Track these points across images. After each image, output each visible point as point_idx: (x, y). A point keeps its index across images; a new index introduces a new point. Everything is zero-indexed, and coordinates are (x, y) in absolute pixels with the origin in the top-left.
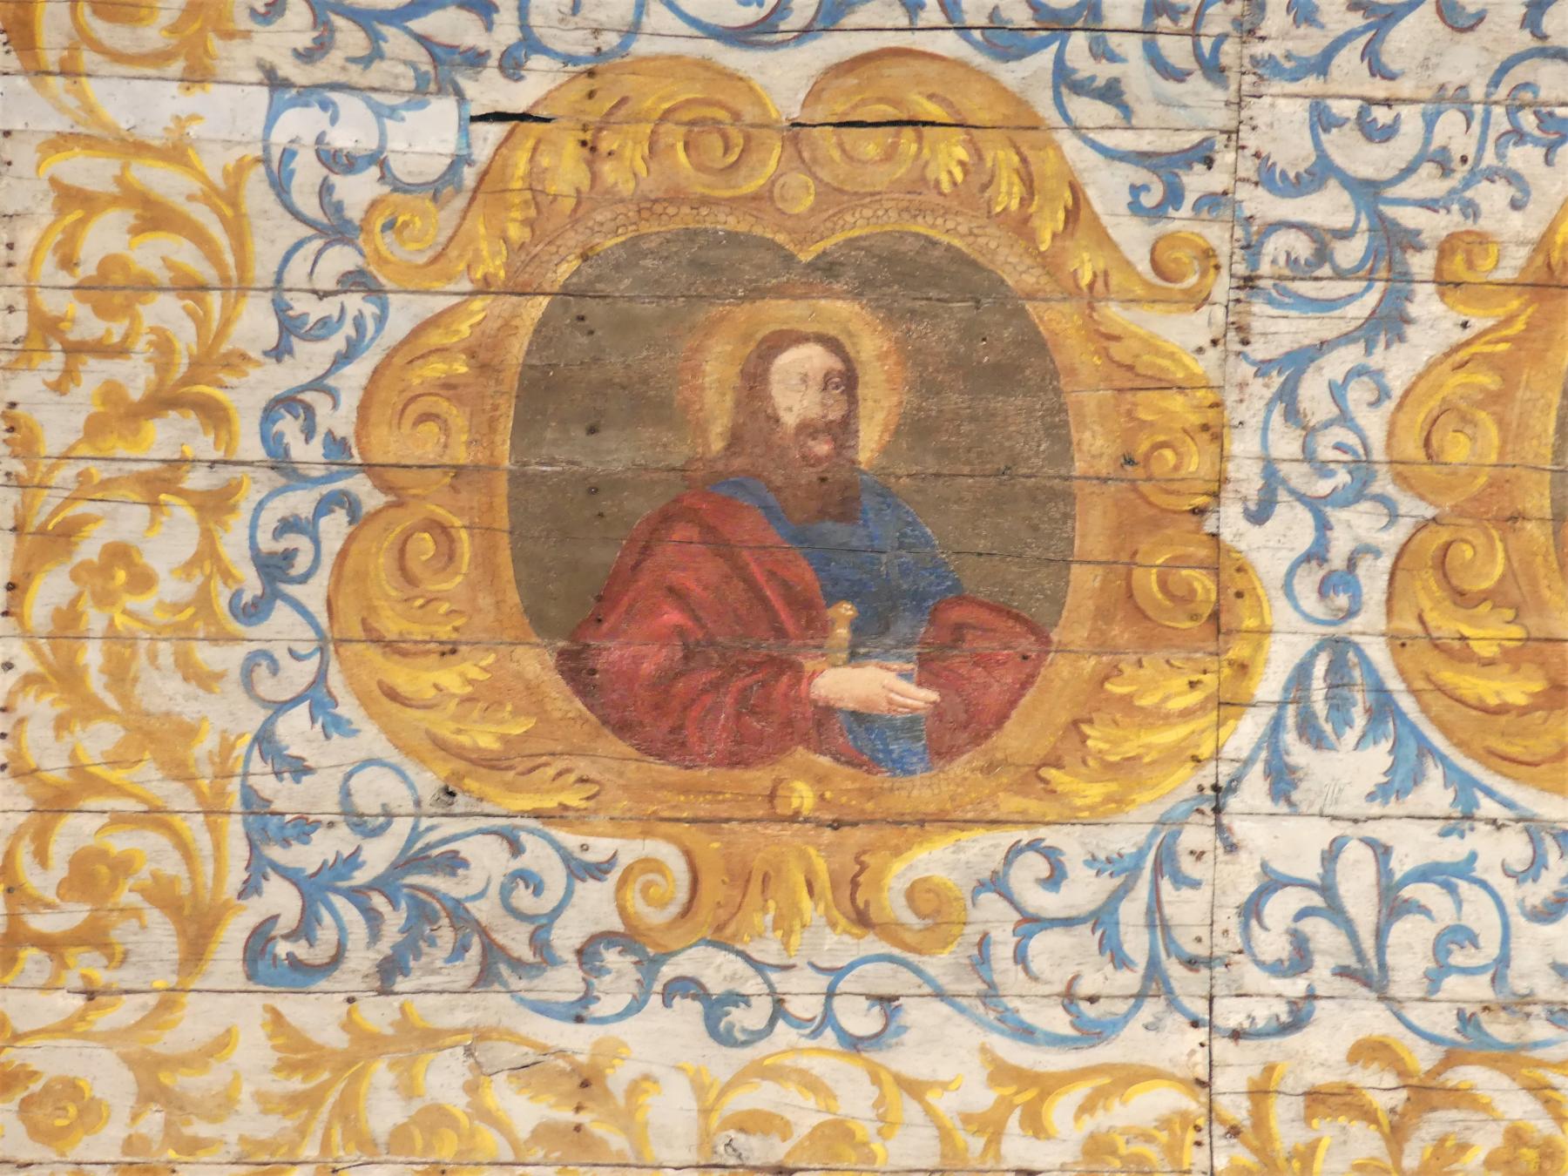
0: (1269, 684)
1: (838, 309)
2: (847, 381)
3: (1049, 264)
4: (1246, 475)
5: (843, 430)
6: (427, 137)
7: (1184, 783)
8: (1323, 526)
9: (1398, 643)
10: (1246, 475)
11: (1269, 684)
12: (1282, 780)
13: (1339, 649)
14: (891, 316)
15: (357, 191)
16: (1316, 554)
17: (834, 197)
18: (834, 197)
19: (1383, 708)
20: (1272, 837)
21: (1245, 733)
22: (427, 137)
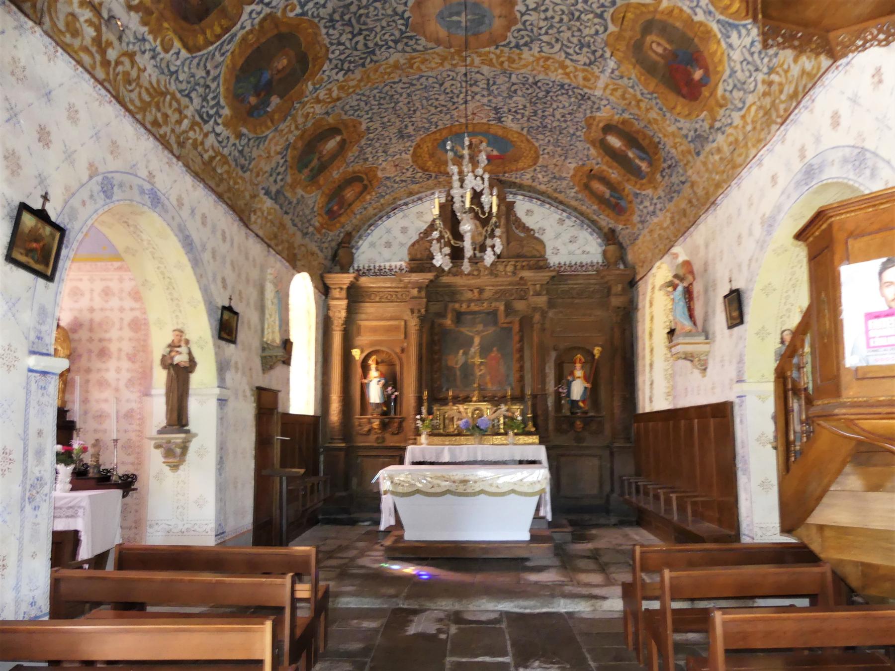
0: (719, 36)
1: (649, 39)
2: (659, 44)
3: (649, 12)
4: (689, 11)
5: (665, 49)
6: (612, 64)
7: (726, 58)
8: (701, 7)
9: (722, 13)
10: (689, 11)
11: (719, 36)
12: (730, 46)
13: (718, 21)
14: (651, 33)
15: (616, 73)
16: (705, 12)
17: (632, 29)
18: (632, 29)
19: (730, 25)
20: (736, 56)
21: (723, 43)
22: (612, 64)
